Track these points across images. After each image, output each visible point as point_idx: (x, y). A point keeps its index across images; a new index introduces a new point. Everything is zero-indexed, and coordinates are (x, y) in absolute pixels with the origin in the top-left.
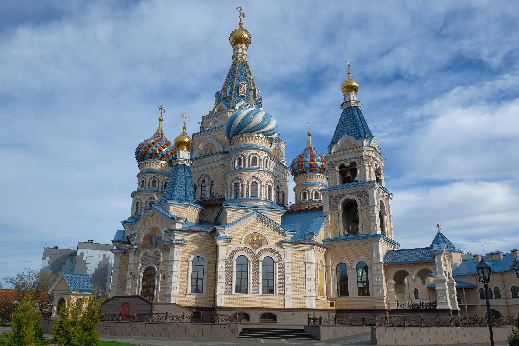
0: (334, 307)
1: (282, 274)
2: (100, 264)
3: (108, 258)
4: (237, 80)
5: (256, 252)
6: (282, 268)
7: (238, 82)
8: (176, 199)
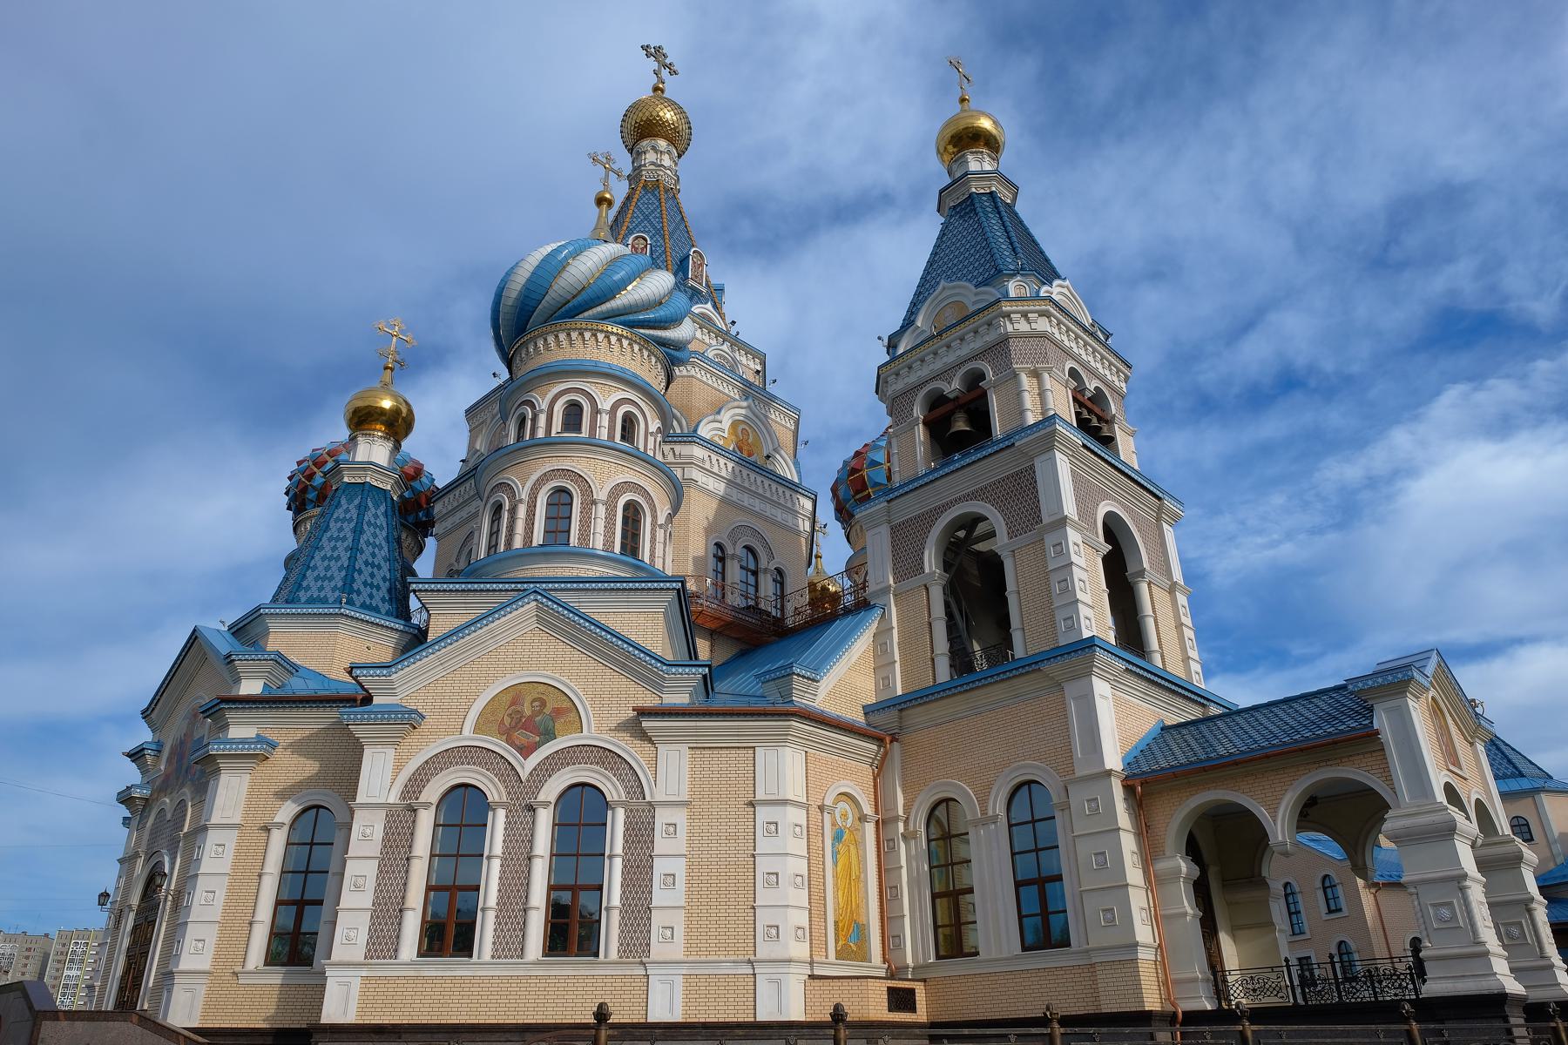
0: (913, 1009)
1: (641, 861)
5: (526, 767)
6: (641, 834)
8: (303, 600)
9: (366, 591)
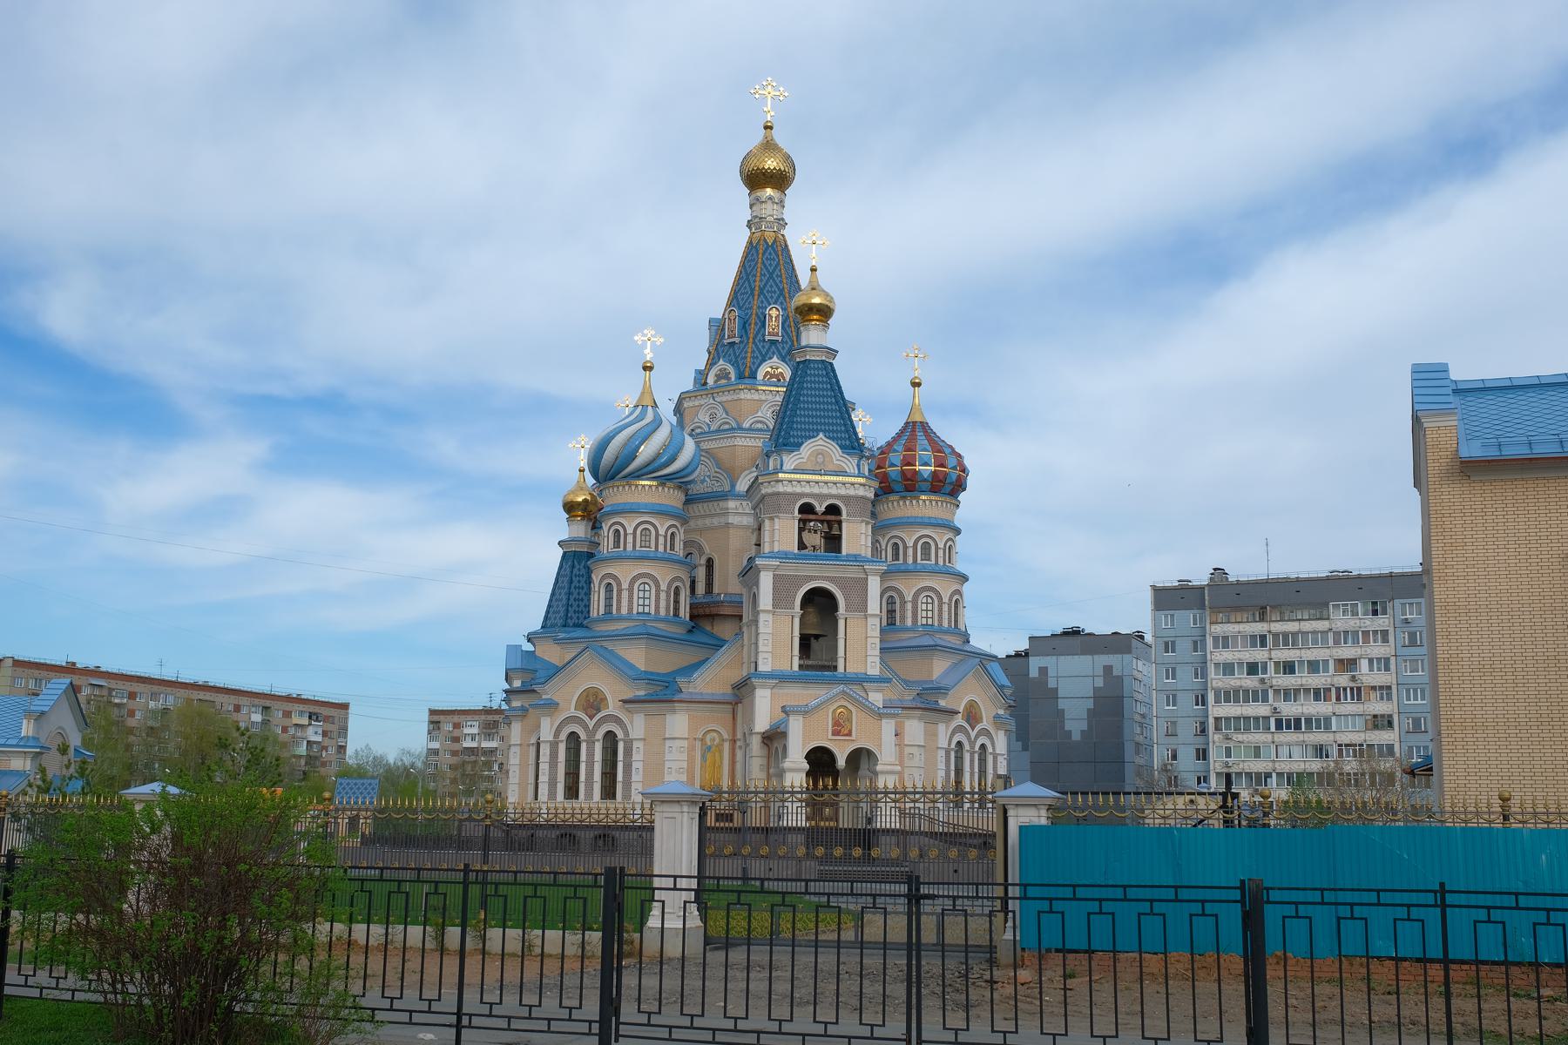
0: (732, 821)
2: (1098, 696)
3: (1118, 676)
4: (759, 296)
7: (762, 302)
9: (575, 616)
